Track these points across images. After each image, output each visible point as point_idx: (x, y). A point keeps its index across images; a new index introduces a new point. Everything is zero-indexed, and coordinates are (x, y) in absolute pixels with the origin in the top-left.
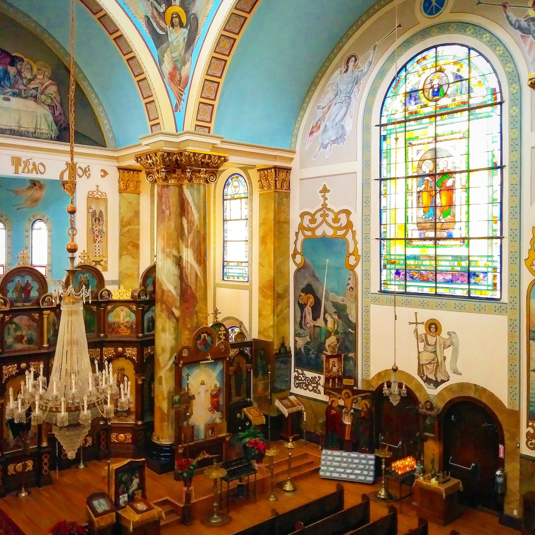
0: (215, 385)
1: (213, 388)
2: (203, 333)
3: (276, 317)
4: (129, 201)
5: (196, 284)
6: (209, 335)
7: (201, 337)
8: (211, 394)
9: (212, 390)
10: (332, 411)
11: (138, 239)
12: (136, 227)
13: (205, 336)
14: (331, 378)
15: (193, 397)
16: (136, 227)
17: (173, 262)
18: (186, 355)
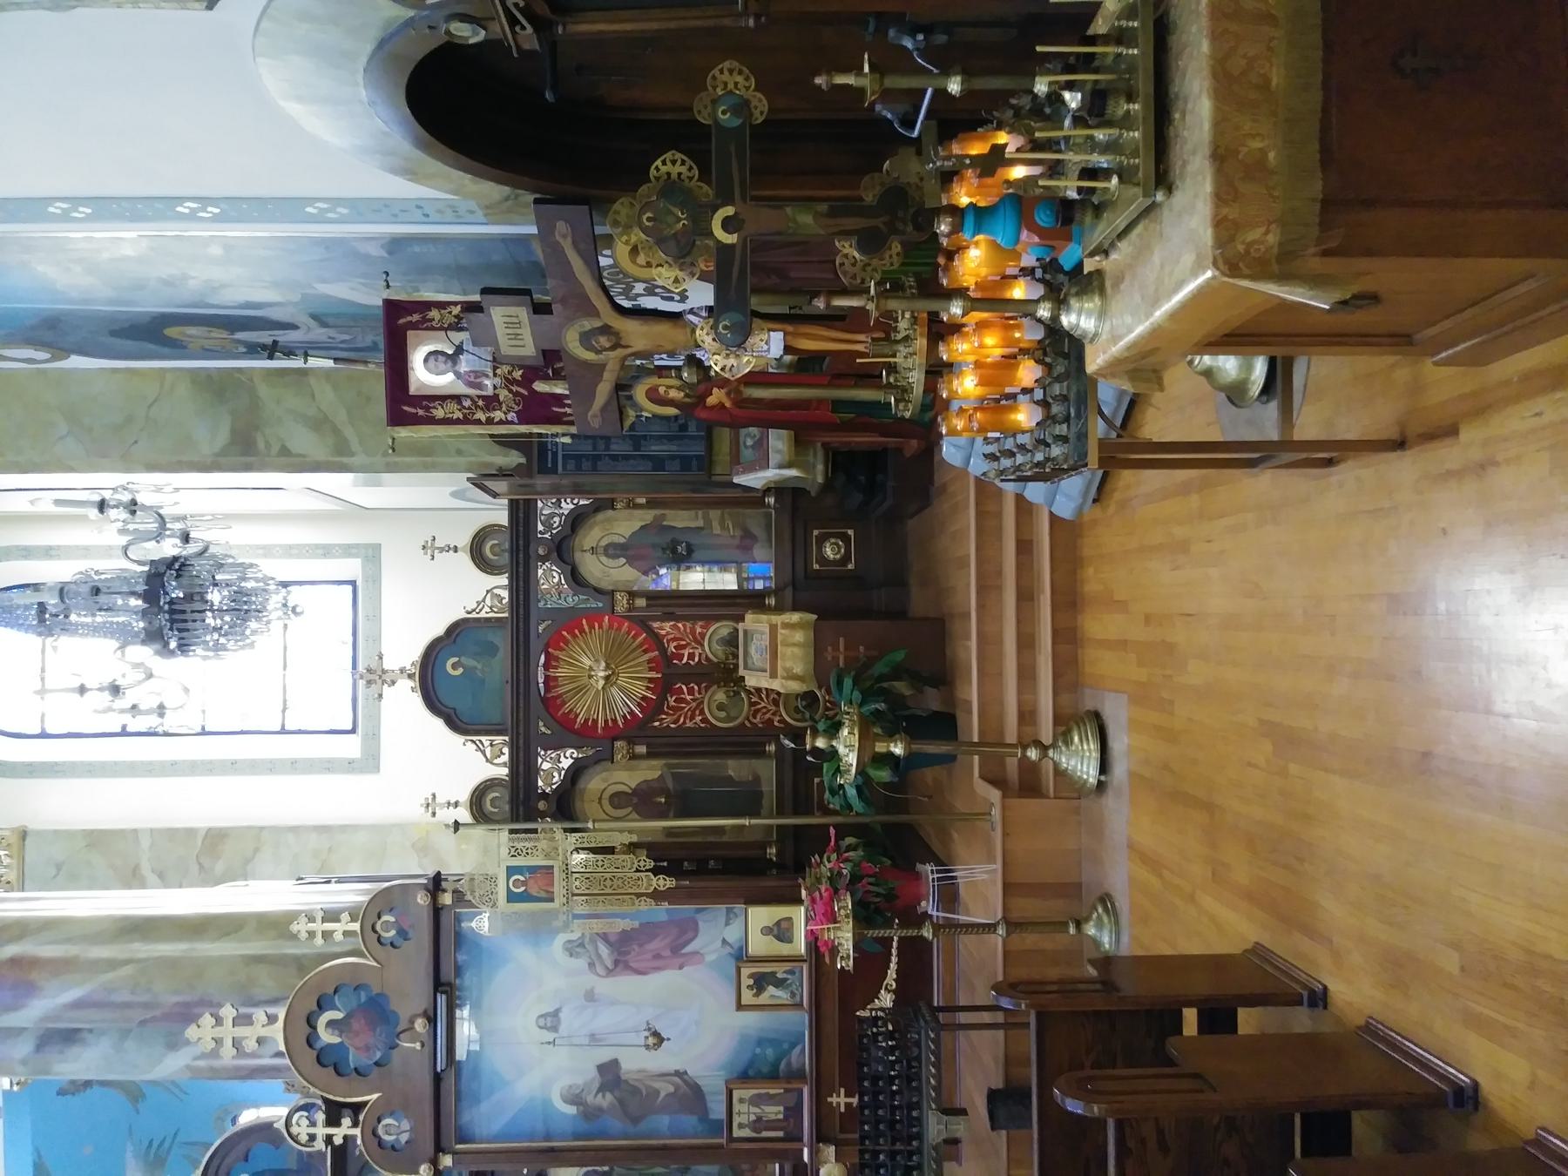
0: (572, 949)
1: (581, 963)
2: (311, 1041)
3: (345, 460)
4: (54, 872)
5: (127, 1005)
6: (322, 1005)
7: (330, 1046)
8: (610, 972)
9: (591, 965)
10: (711, 400)
11: (191, 832)
12: (145, 843)
13: (331, 1024)
14: (527, 381)
15: (610, 1074)
16: (145, 843)
17: (61, 1052)
18: (406, 1125)
